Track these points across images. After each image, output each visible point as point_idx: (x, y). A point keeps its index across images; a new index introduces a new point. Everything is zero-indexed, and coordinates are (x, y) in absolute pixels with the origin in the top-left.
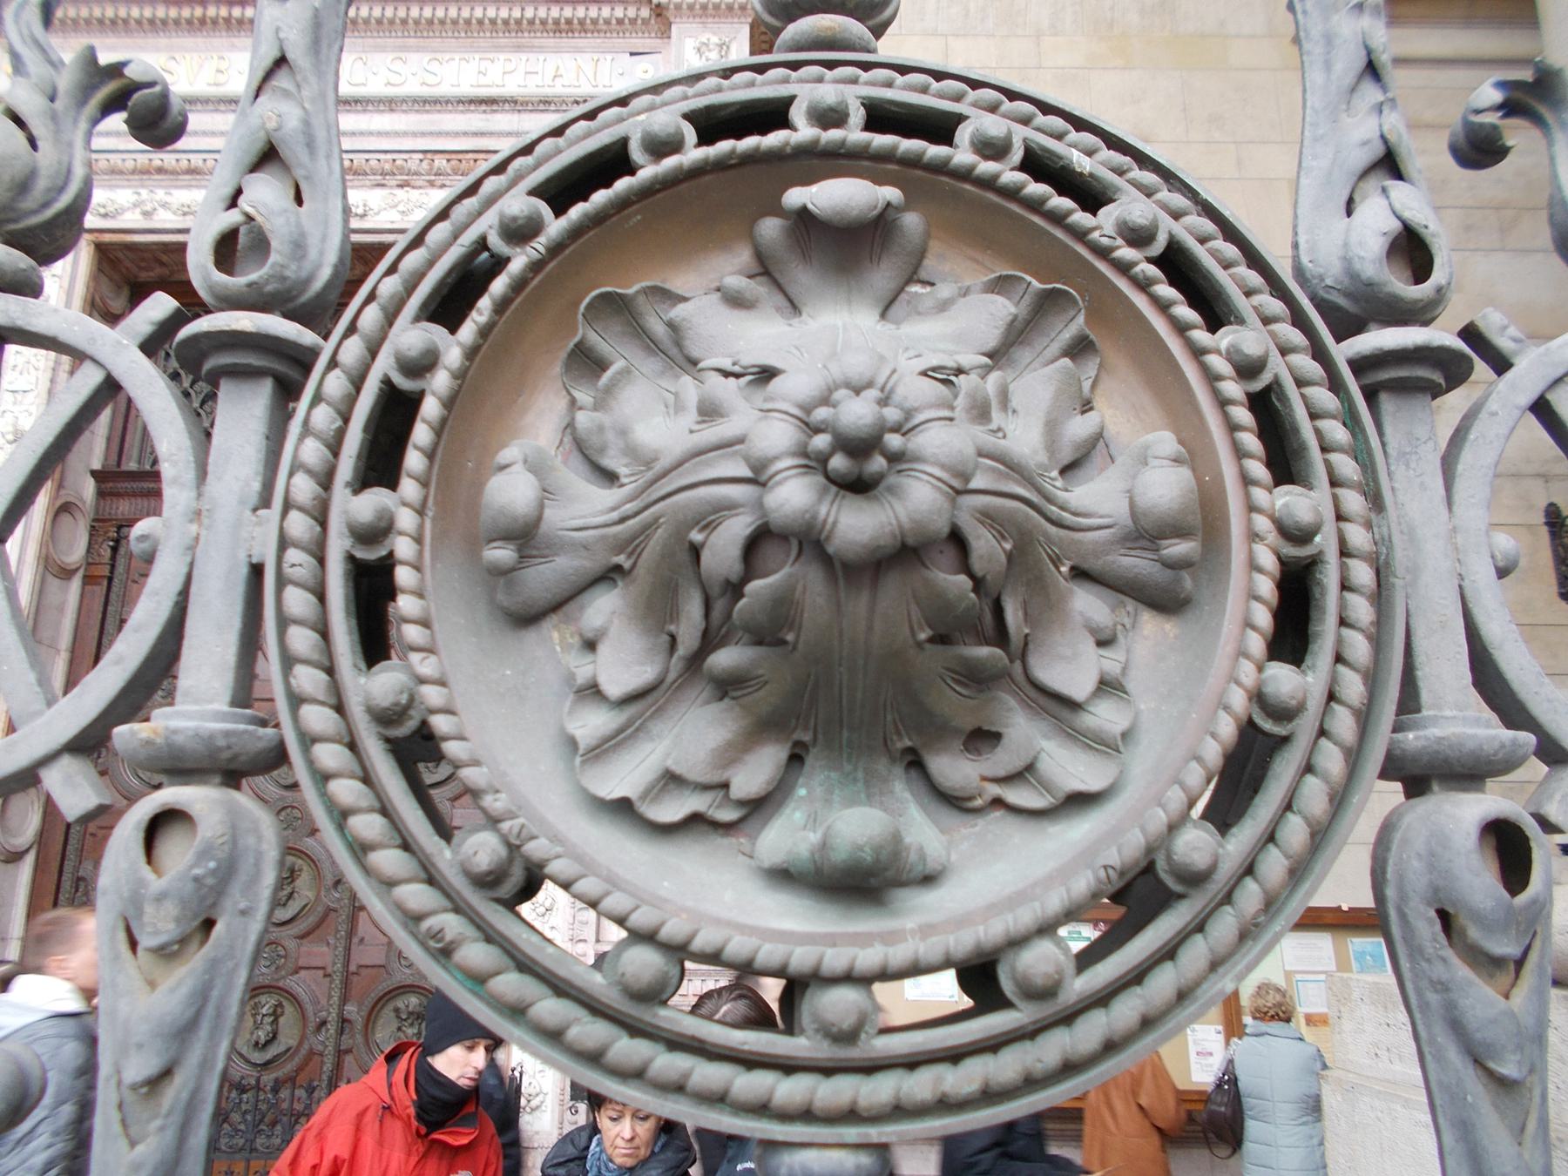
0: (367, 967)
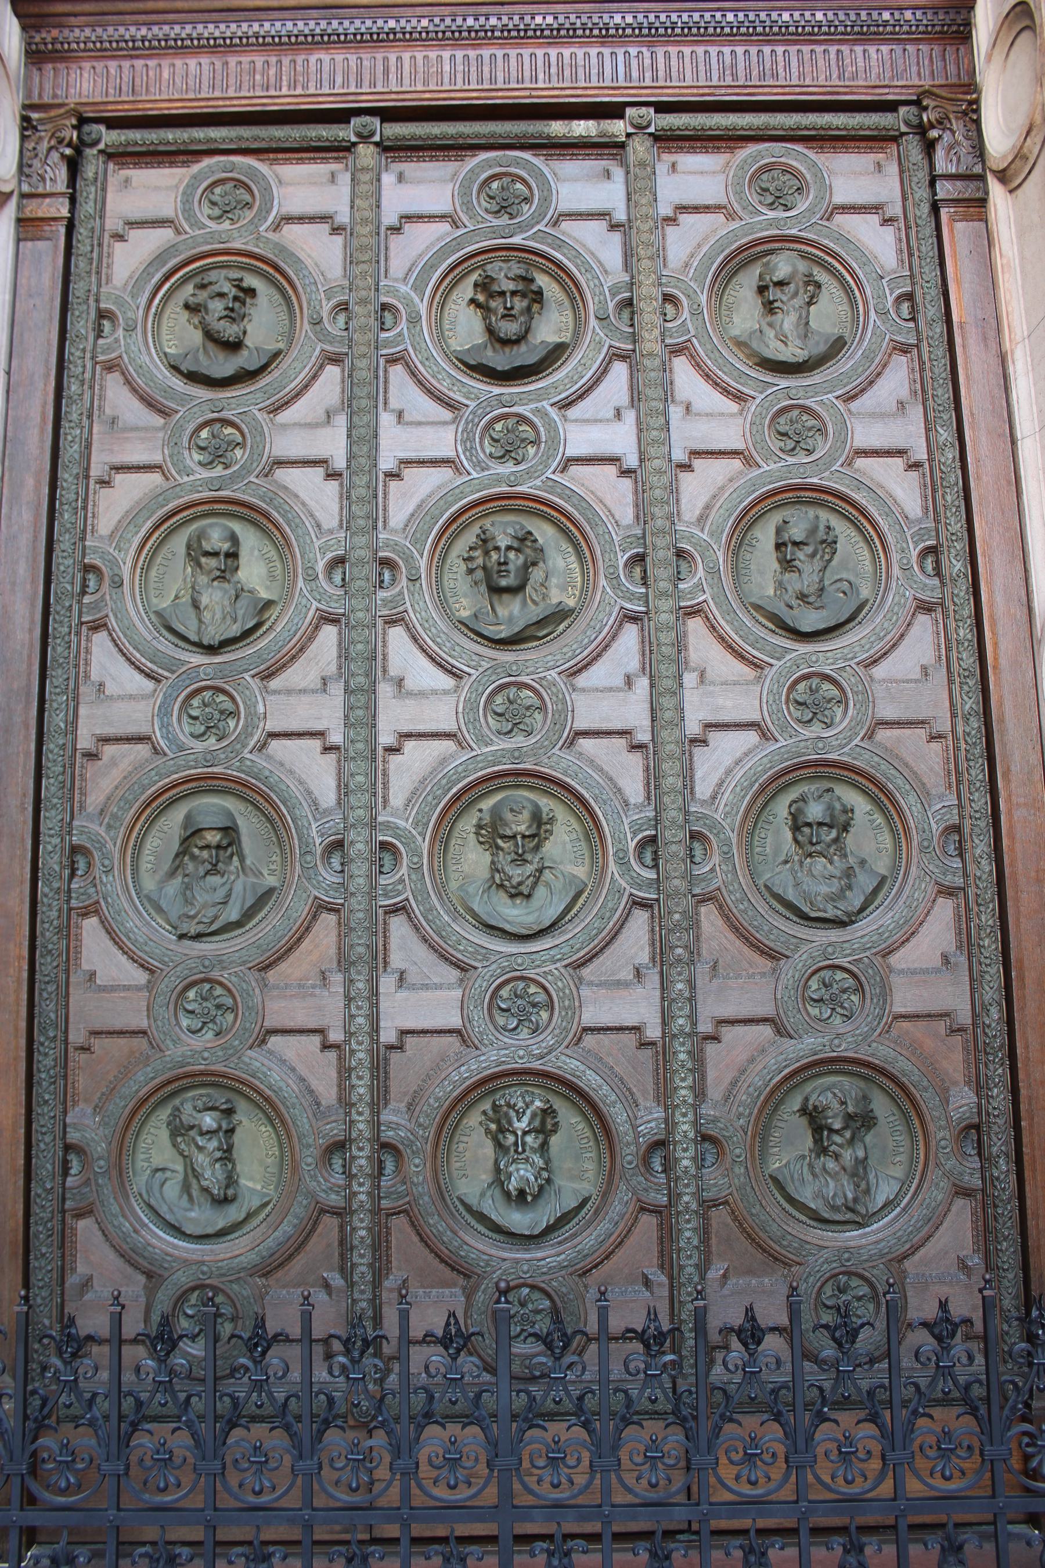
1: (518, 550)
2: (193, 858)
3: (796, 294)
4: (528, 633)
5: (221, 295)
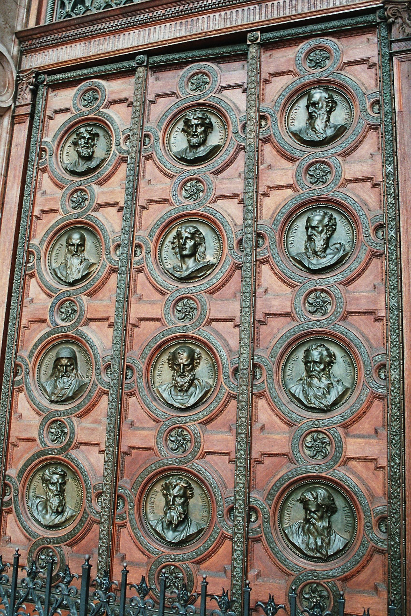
0: (270, 455)
4: (193, 275)
5: (84, 138)
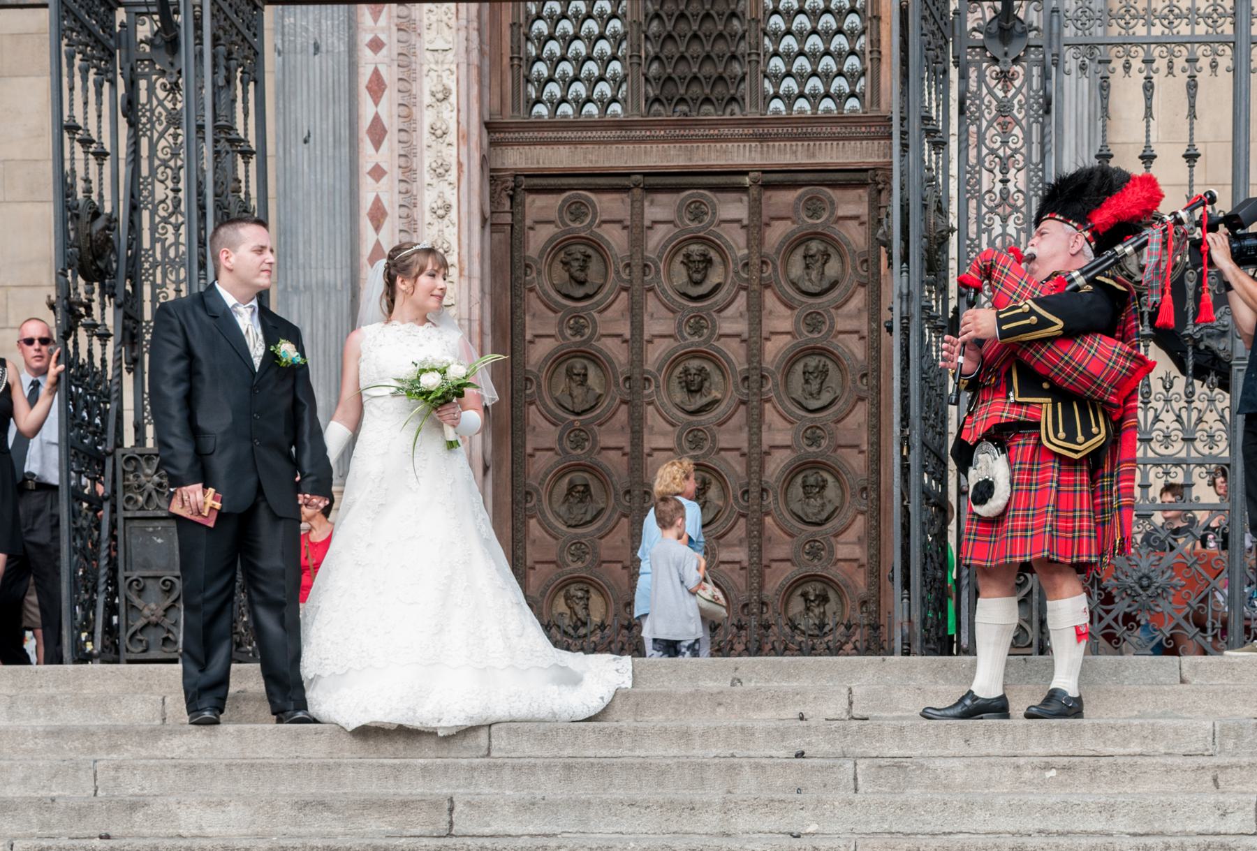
1: (699, 375)
2: (573, 496)
3: (817, 261)
5: (577, 259)
